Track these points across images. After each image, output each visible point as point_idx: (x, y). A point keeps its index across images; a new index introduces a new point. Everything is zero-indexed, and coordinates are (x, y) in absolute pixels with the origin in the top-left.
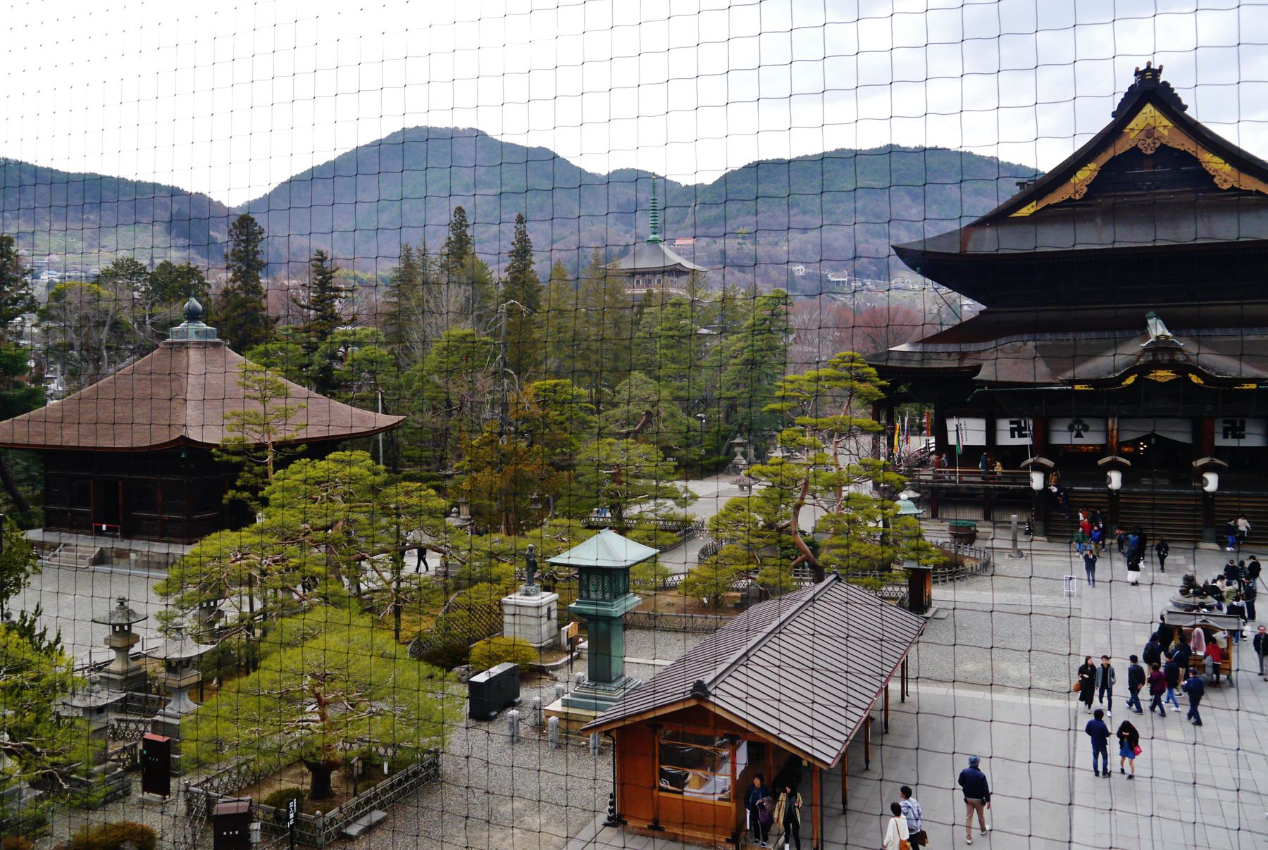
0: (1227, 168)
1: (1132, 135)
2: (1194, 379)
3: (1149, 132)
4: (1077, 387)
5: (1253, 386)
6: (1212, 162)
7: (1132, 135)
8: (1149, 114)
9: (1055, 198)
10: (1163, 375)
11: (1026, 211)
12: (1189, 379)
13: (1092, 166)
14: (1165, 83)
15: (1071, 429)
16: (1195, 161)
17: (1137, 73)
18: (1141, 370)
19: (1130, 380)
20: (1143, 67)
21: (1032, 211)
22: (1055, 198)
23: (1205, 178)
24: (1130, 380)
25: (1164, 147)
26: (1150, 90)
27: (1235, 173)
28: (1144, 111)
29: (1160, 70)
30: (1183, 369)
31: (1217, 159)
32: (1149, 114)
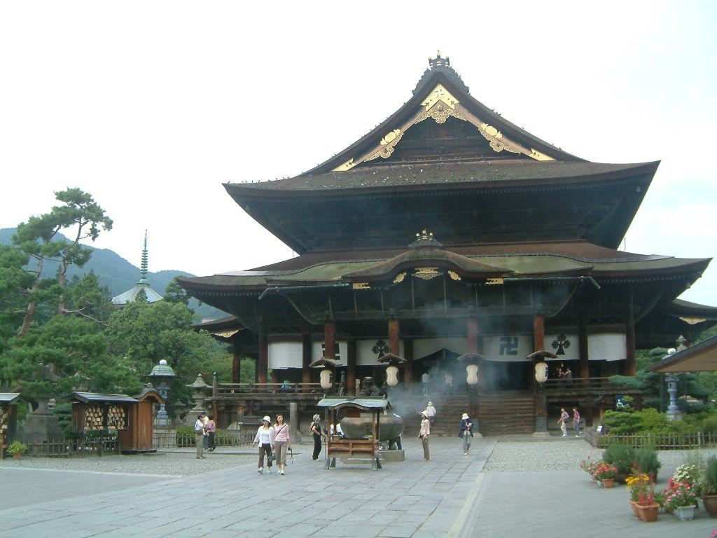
0: (499, 135)
1: (427, 108)
2: (455, 276)
3: (441, 106)
4: (356, 286)
5: (500, 281)
6: (489, 131)
7: (427, 108)
8: (441, 95)
9: (369, 157)
10: (427, 273)
11: (344, 168)
12: (449, 276)
13: (397, 132)
14: (452, 70)
15: (375, 350)
16: (475, 130)
17: (430, 61)
18: (409, 268)
19: (400, 278)
20: (434, 57)
21: (350, 167)
22: (369, 157)
23: (484, 143)
24: (400, 278)
25: (451, 118)
26: (440, 75)
27: (506, 140)
28: (436, 90)
29: (448, 59)
30: (445, 266)
31: (491, 127)
32: (441, 95)
